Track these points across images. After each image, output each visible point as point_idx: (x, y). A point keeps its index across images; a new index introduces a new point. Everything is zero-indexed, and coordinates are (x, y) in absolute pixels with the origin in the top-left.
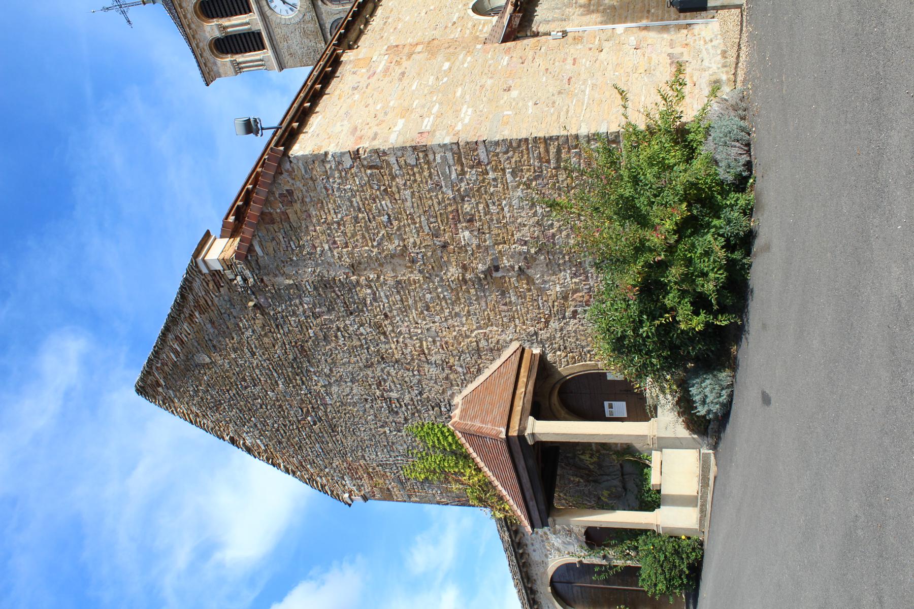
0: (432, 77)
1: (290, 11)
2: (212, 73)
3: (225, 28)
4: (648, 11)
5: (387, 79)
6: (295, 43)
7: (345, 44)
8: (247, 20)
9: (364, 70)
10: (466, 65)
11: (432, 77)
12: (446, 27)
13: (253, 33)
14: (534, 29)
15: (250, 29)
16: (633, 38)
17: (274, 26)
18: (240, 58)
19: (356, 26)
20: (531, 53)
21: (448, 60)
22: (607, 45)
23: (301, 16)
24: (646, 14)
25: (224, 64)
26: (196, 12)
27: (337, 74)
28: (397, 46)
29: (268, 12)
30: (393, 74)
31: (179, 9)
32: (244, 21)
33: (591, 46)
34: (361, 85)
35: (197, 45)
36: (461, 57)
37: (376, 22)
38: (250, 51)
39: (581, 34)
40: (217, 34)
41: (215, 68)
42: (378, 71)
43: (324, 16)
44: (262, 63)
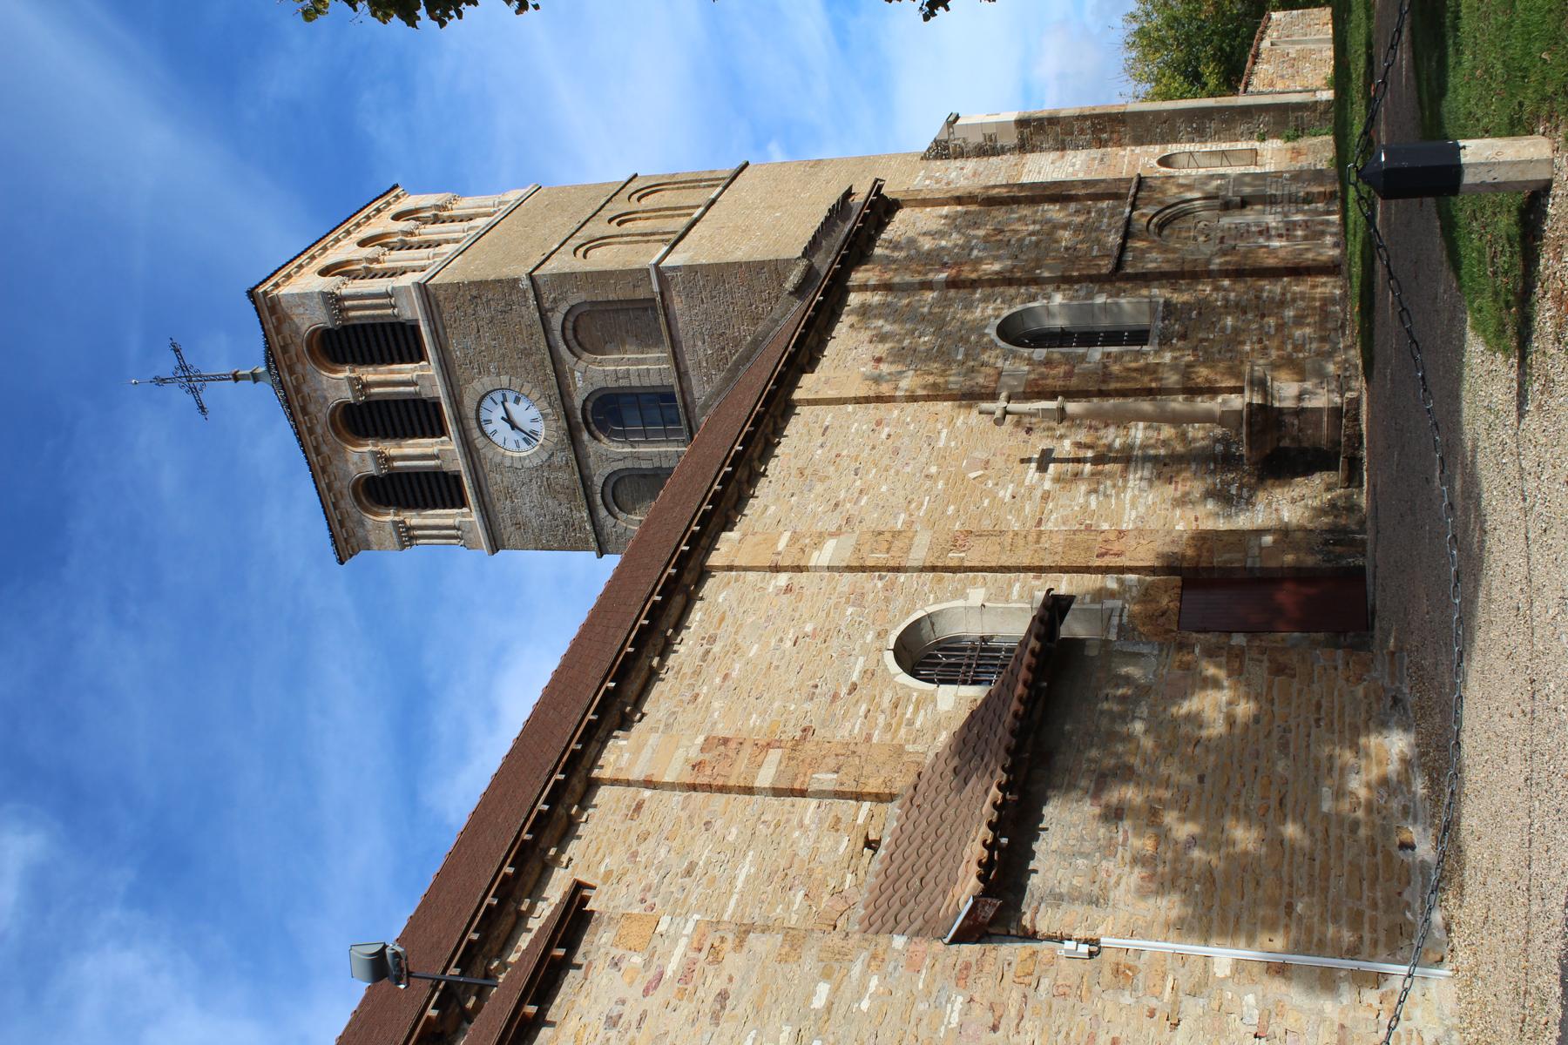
0: (787, 1029)
1: (523, 445)
2: (353, 540)
3: (389, 459)
4: (1290, 908)
5: (686, 1008)
6: (529, 503)
7: (614, 716)
8: (435, 450)
9: (637, 960)
10: (865, 1005)
11: (787, 1029)
12: (835, 696)
13: (445, 474)
14: (1026, 921)
15: (440, 467)
16: (1250, 999)
17: (487, 468)
18: (413, 518)
19: (643, 663)
20: (1016, 995)
21: (826, 975)
22: (1192, 1008)
23: (545, 456)
24: (1284, 920)
25: (380, 527)
26: (333, 424)
27: (578, 959)
28: (725, 741)
29: (480, 442)
30: (701, 993)
31: (300, 417)
32: (429, 451)
33: (1154, 1003)
34: (626, 1010)
35: (330, 487)
36: (857, 970)
37: (687, 647)
38: (435, 507)
39: (1130, 960)
40: (371, 469)
41: (360, 532)
42: (669, 973)
43: (592, 460)
44: (457, 534)
